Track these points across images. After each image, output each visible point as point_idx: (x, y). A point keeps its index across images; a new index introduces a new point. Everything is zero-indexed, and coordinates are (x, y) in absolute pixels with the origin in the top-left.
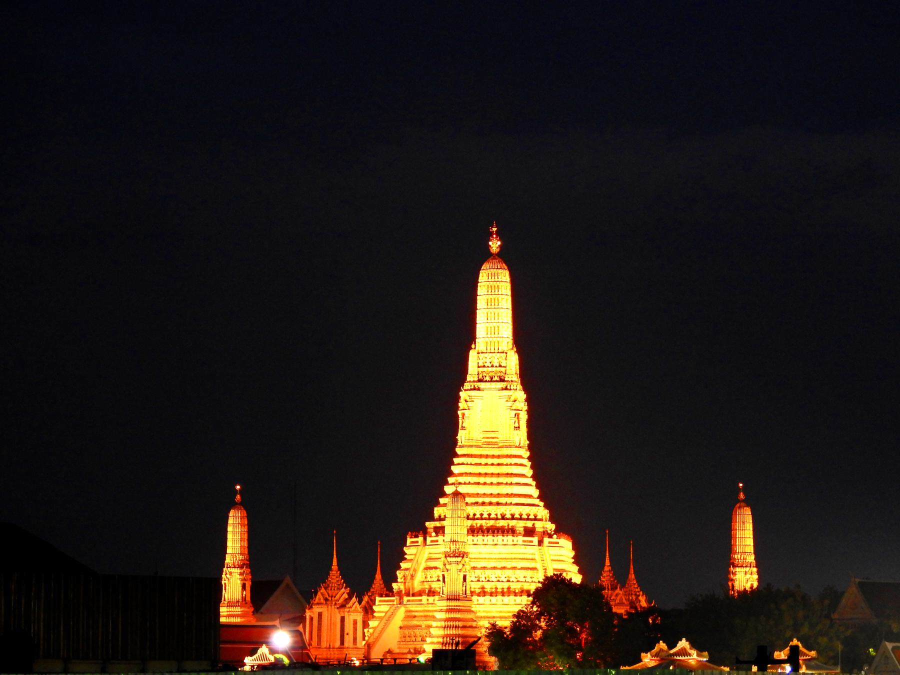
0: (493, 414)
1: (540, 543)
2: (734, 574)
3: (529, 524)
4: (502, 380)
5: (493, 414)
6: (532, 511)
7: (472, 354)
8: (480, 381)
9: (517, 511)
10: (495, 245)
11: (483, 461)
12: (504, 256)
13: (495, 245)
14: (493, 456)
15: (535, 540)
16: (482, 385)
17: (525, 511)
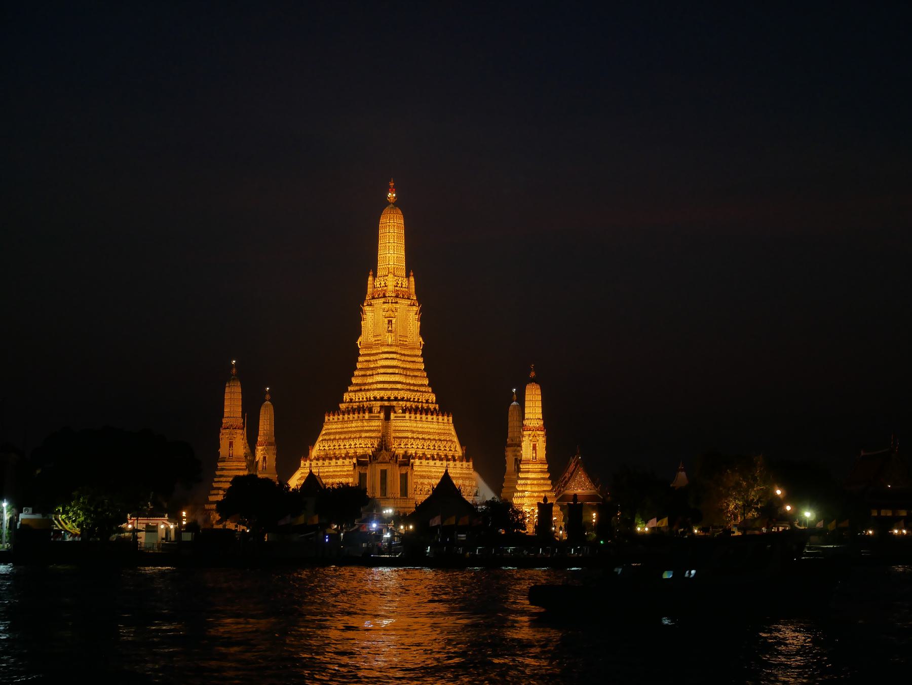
0: (390, 322)
1: (387, 418)
2: (523, 436)
3: (386, 403)
4: (384, 296)
5: (390, 322)
6: (427, 396)
7: (370, 278)
8: (373, 298)
9: (378, 394)
10: (391, 195)
11: (372, 358)
12: (398, 204)
13: (391, 195)
14: (408, 355)
15: (382, 415)
16: (373, 302)
17: (385, 394)
